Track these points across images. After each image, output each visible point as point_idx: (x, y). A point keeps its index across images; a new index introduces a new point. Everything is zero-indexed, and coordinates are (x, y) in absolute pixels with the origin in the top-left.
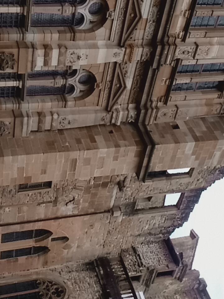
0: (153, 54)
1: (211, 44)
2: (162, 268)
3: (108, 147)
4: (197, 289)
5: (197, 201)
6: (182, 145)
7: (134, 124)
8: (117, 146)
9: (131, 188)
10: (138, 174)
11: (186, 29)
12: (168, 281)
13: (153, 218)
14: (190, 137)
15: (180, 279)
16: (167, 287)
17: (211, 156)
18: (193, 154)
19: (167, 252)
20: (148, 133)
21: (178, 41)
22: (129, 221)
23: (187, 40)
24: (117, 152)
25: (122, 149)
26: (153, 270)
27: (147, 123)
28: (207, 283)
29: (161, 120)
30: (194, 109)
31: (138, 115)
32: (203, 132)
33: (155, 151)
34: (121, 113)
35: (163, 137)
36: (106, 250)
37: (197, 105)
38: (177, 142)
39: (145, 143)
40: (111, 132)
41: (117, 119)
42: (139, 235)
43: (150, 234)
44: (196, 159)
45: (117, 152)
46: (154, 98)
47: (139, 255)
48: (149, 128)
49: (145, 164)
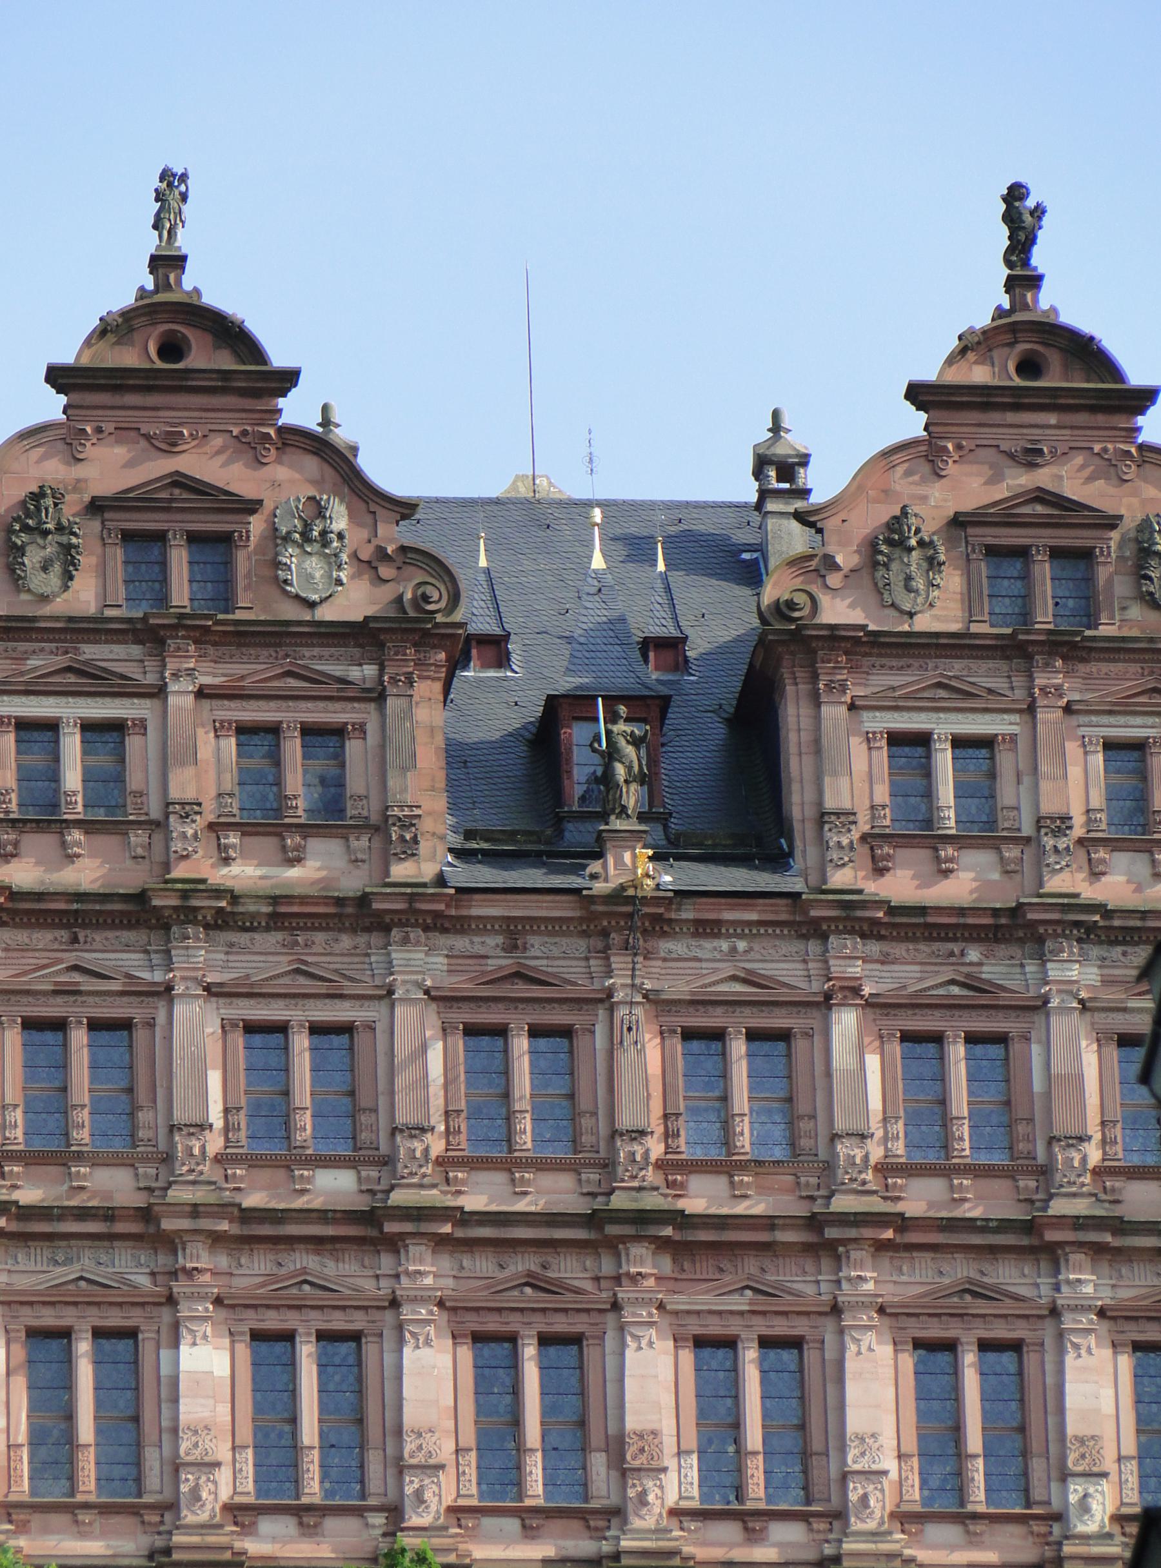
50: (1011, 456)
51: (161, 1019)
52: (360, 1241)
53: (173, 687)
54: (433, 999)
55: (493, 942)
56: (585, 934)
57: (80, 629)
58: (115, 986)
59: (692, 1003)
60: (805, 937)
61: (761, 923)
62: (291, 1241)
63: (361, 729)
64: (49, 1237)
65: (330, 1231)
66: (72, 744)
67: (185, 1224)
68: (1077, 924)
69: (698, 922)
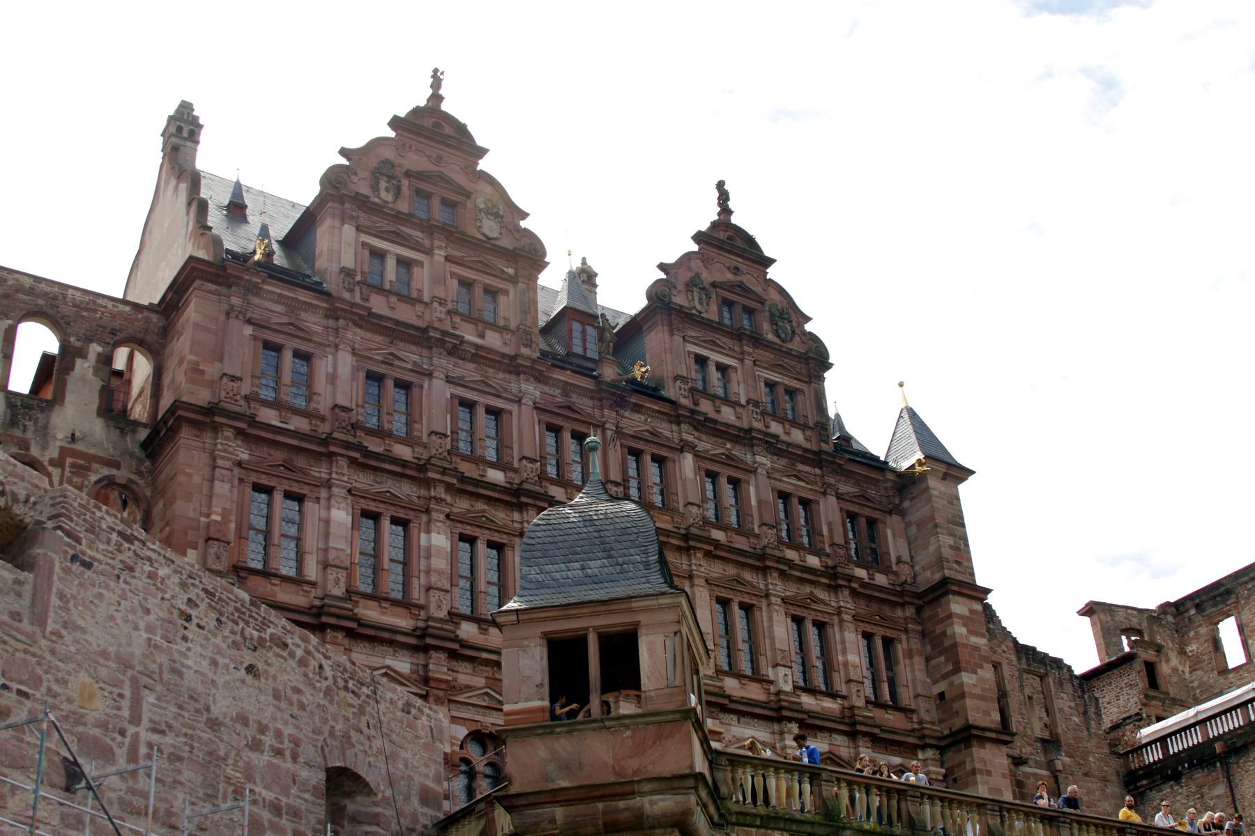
0: (865, 734)
1: (846, 664)
2: (1141, 683)
3: (976, 783)
4: (1175, 617)
5: (1033, 649)
6: (966, 689)
7: (942, 750)
8: (973, 772)
9: (1022, 747)
10: (1006, 743)
11: (833, 695)
12: (1164, 669)
13: (1061, 710)
14: (954, 678)
15: (1159, 649)
16: (1175, 670)
17: (976, 648)
18: (975, 672)
19: (1116, 671)
20: (952, 734)
21: (846, 704)
22: (1069, 745)
23: (844, 693)
24: (981, 772)
25: (977, 766)
26: (1146, 696)
27: (939, 734)
28: (1162, 601)
29: (935, 715)
30: (917, 673)
31: (931, 746)
32: (947, 661)
33: (976, 723)
34: (931, 768)
35: (957, 713)
36: (1114, 778)
37: (913, 671)
38: (962, 696)
39: (966, 736)
40: (955, 780)
41: (937, 773)
42: (1088, 729)
43: (1085, 713)
44: (982, 667)
45: (981, 772)
46: (909, 726)
47: (1124, 719)
48: (946, 732)
49: (993, 735)
50: (728, 268)
51: (426, 386)
52: (506, 503)
53: (436, 251)
54: (536, 408)
55: (557, 392)
56: (592, 398)
57: (399, 217)
58: (409, 366)
59: (633, 436)
60: (671, 422)
61: (658, 412)
62: (478, 496)
63: (506, 292)
64: (375, 469)
65: (496, 495)
66: (391, 263)
67: (438, 476)
68: (767, 442)
69: (635, 404)
